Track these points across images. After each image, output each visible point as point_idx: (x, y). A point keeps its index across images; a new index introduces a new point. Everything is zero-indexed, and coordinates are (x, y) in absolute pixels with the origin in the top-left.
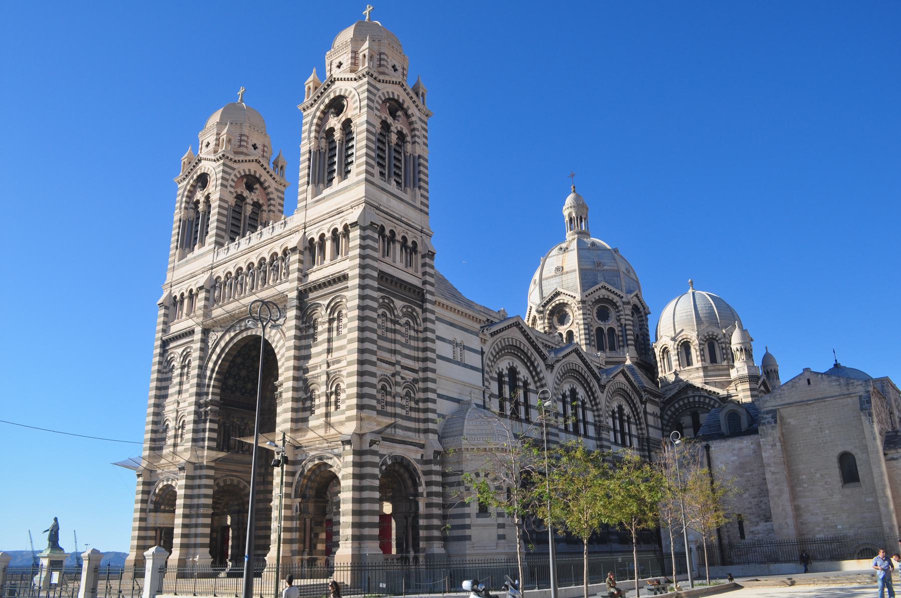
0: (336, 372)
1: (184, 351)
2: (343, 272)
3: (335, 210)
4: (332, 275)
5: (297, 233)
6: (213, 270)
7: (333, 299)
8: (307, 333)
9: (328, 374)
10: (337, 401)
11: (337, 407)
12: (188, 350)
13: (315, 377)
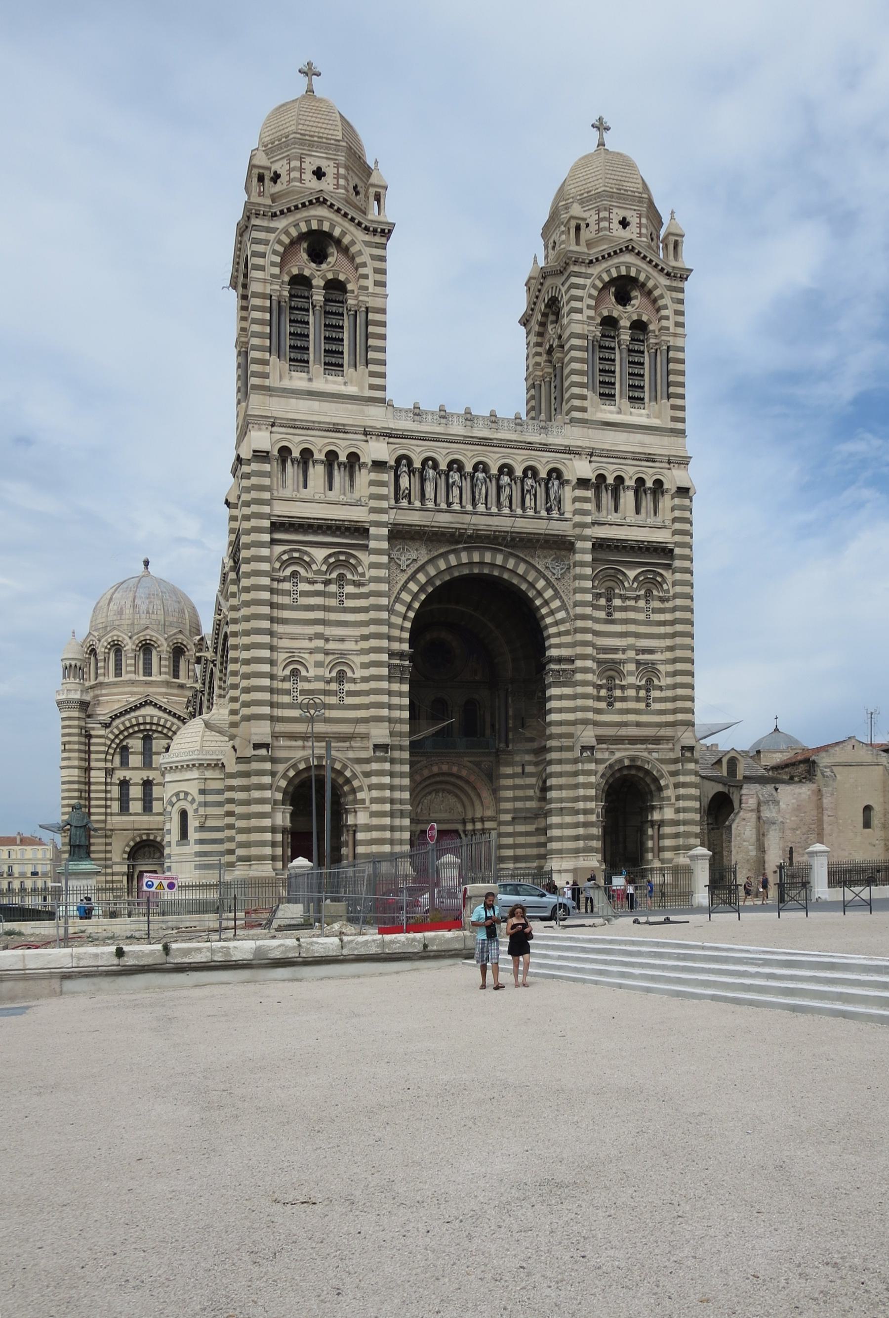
0: (648, 664)
1: (330, 556)
2: (664, 545)
3: (645, 454)
4: (648, 542)
5: (577, 456)
6: (391, 440)
7: (643, 571)
8: (598, 603)
9: (638, 663)
10: (648, 697)
11: (648, 705)
12: (342, 558)
13: (616, 663)
